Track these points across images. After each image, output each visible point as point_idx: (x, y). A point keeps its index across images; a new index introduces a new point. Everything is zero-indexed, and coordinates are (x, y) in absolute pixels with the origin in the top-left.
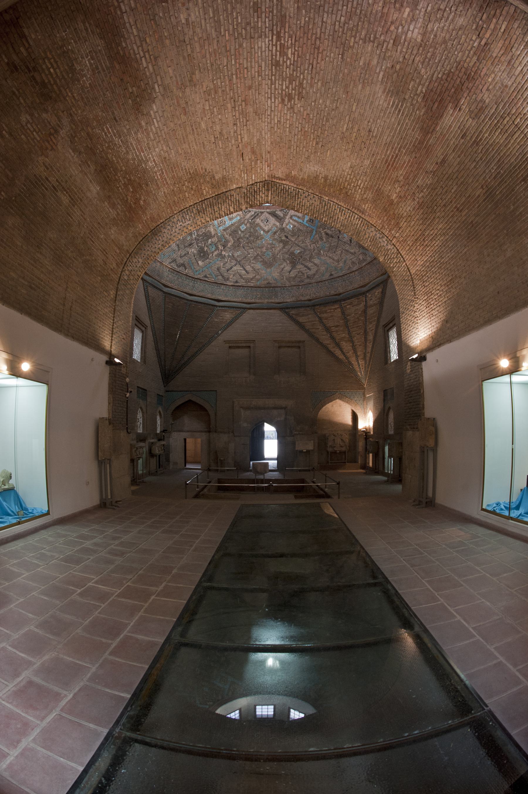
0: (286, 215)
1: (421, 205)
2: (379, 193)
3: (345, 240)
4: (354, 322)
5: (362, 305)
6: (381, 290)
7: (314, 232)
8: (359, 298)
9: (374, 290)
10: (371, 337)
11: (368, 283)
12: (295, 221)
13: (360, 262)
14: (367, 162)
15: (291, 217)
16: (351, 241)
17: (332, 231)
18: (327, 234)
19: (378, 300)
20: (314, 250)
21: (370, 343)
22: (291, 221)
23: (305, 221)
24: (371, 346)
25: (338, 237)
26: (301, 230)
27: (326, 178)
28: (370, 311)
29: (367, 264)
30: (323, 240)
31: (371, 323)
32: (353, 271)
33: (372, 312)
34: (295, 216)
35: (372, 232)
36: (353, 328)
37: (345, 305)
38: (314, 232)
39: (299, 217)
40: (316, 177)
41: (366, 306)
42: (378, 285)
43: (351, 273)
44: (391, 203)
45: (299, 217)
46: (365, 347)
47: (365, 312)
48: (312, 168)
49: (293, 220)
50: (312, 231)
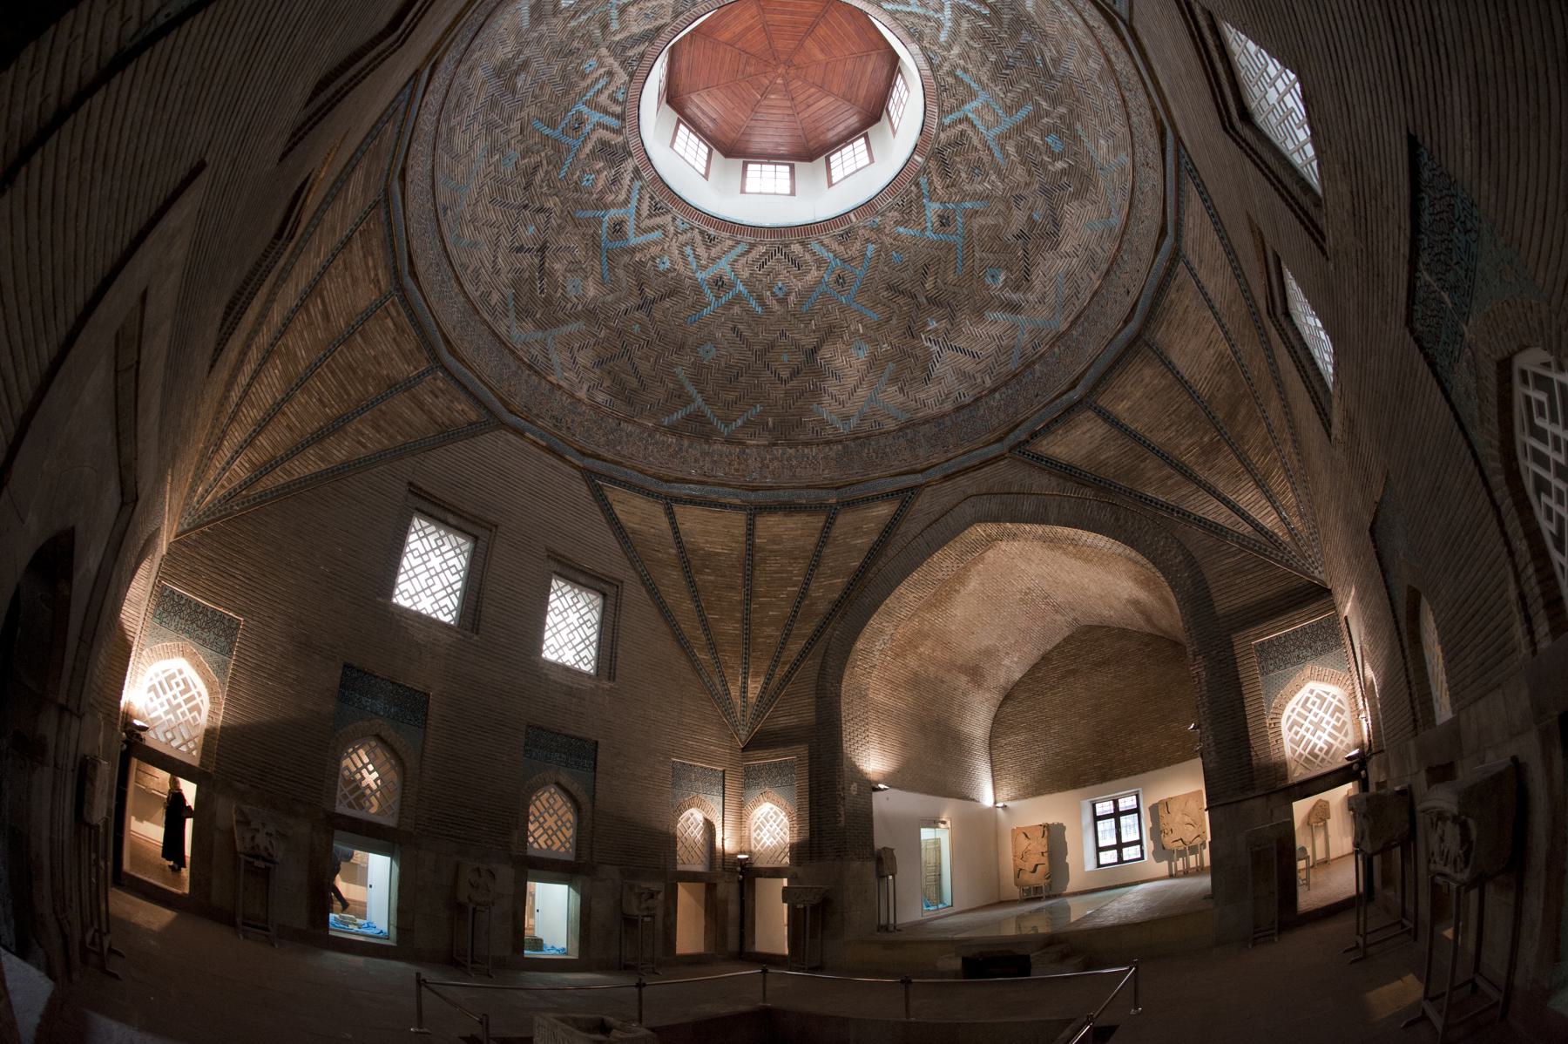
0: (622, 63)
1: (916, 674)
2: (926, 636)
3: (521, 229)
4: (350, 366)
5: (405, 370)
6: (473, 416)
7: (548, 131)
8: (420, 352)
9: (462, 396)
10: (340, 451)
11: (462, 361)
12: (597, 80)
13: (486, 296)
14: (953, 628)
15: (610, 74)
16: (520, 249)
17: (541, 187)
18: (536, 168)
19: (448, 422)
20: (506, 132)
21: (322, 459)
22: (602, 71)
23: (584, 109)
24: (314, 469)
25: (526, 207)
26: (566, 93)
27: (957, 592)
28: (401, 405)
29: (490, 327)
30: (523, 158)
31: (378, 428)
32: (461, 285)
33: (407, 413)
34: (608, 83)
35: (889, 630)
36: (333, 372)
37: (392, 309)
38: (548, 131)
39: (600, 91)
40: (963, 584)
41: (408, 385)
42: (478, 401)
43: (457, 278)
44: (916, 647)
45: (600, 91)
46: (296, 450)
47: (393, 387)
48: (973, 584)
49: (601, 76)
50: (552, 124)
